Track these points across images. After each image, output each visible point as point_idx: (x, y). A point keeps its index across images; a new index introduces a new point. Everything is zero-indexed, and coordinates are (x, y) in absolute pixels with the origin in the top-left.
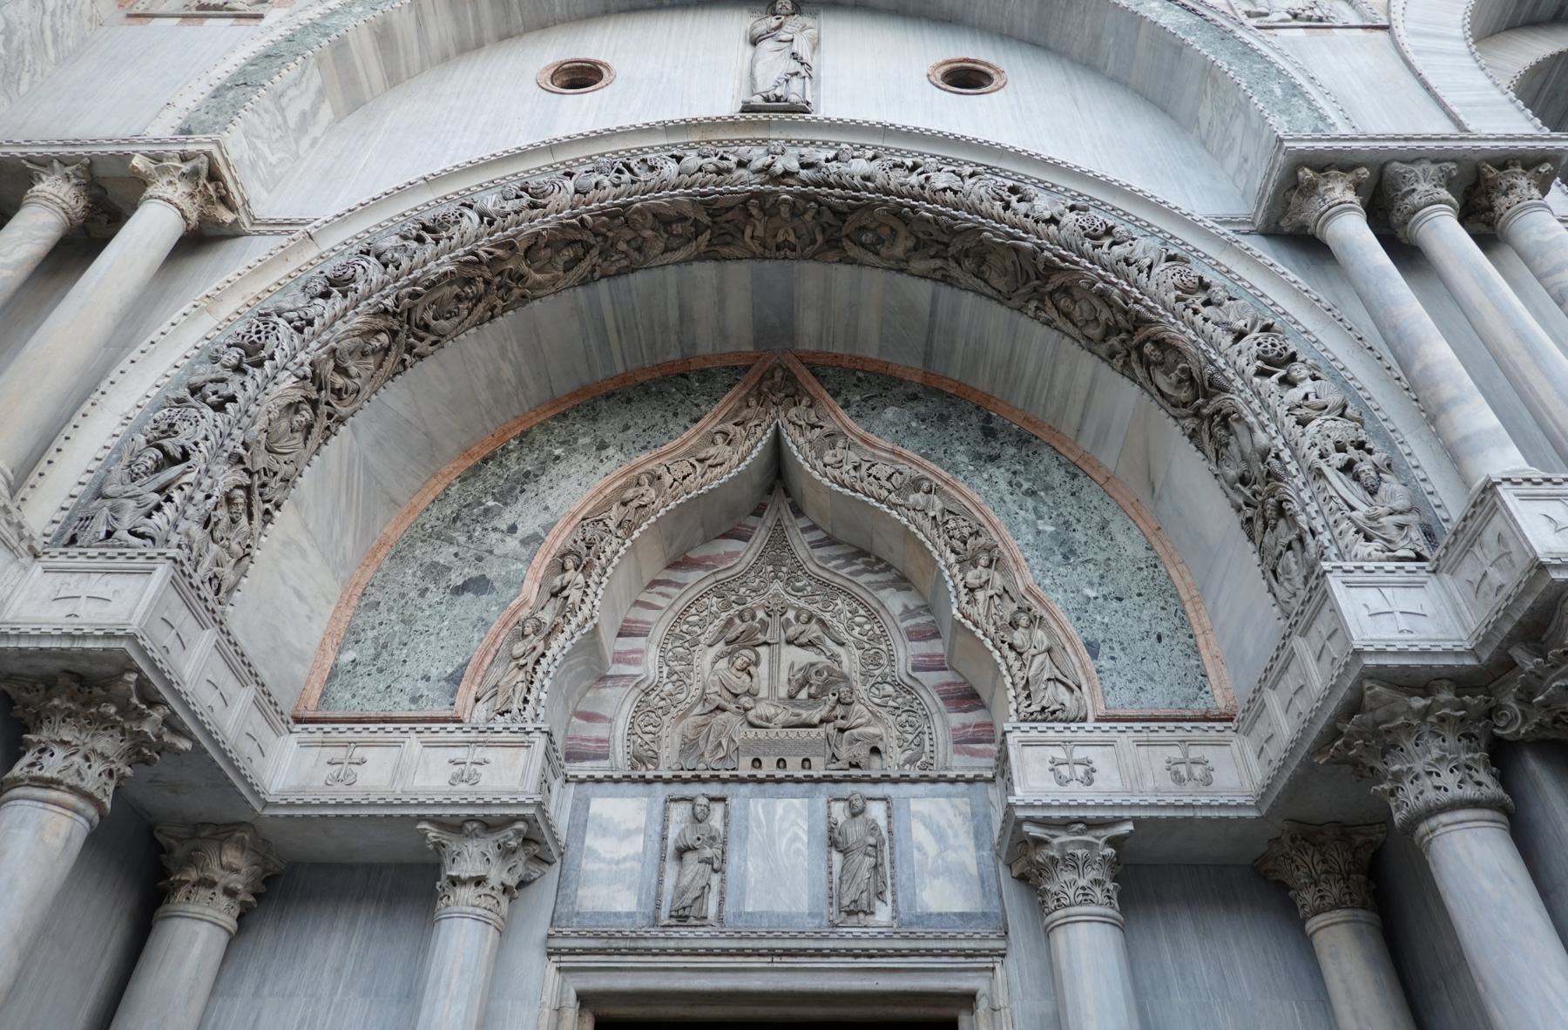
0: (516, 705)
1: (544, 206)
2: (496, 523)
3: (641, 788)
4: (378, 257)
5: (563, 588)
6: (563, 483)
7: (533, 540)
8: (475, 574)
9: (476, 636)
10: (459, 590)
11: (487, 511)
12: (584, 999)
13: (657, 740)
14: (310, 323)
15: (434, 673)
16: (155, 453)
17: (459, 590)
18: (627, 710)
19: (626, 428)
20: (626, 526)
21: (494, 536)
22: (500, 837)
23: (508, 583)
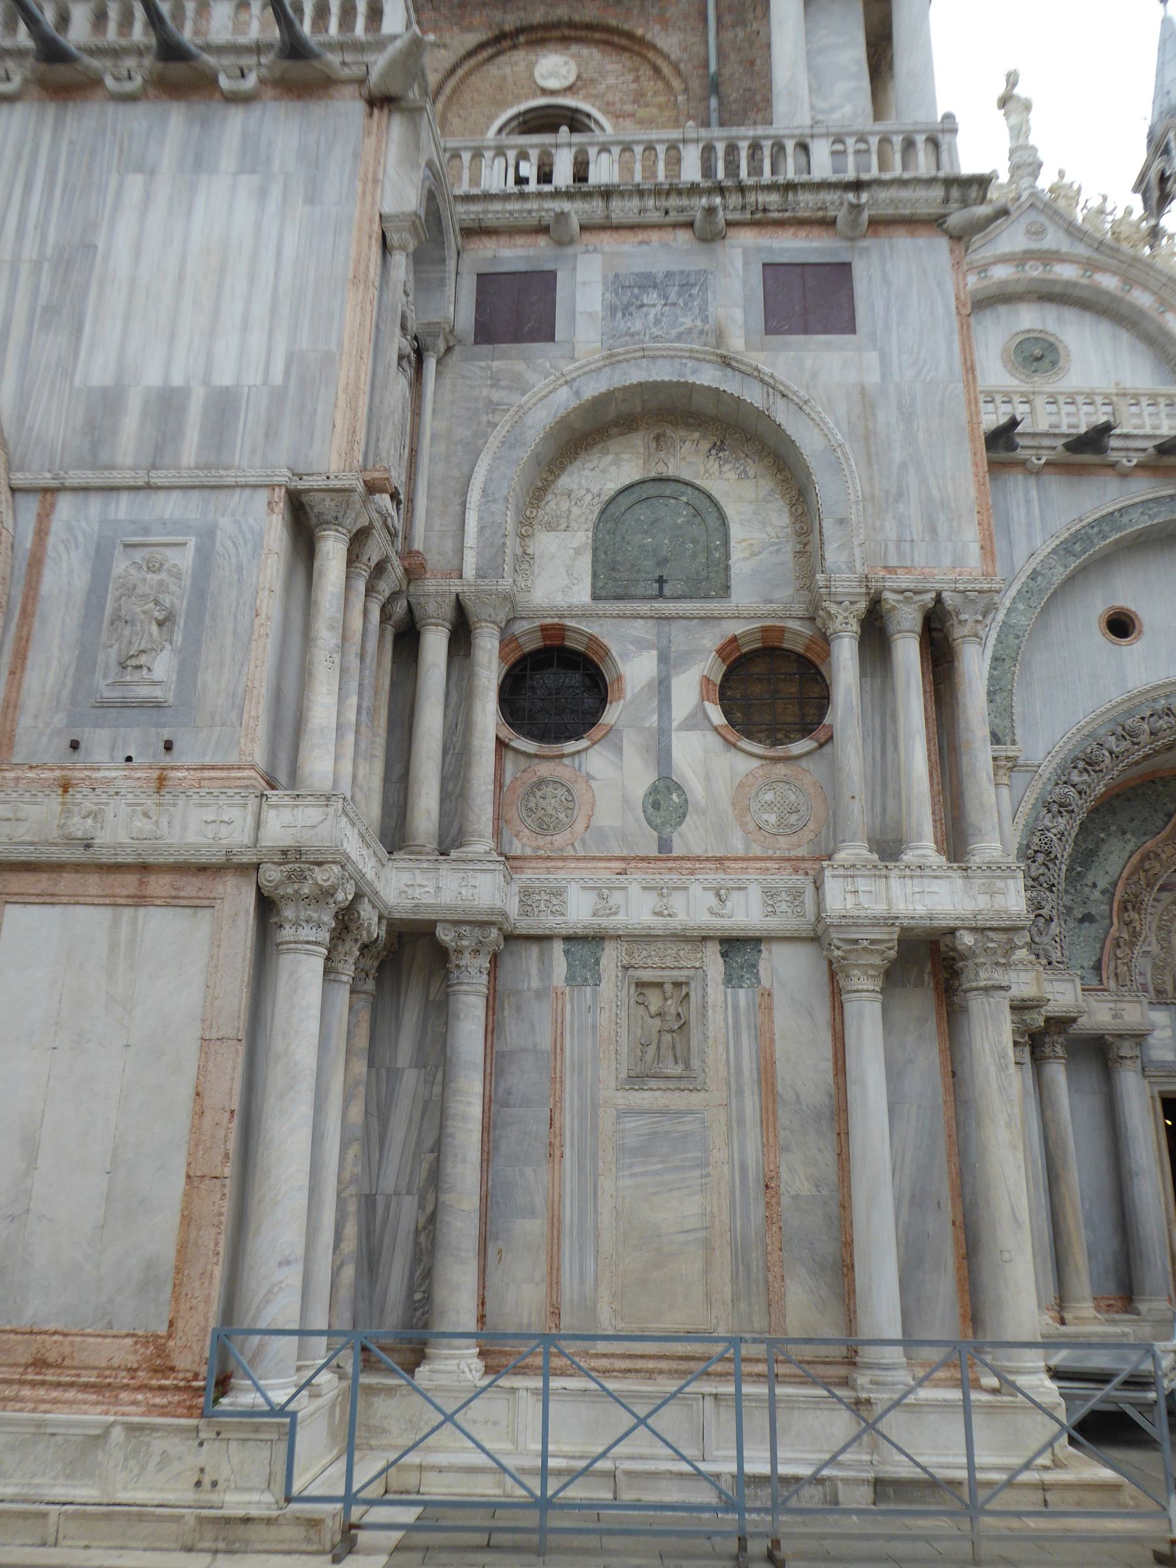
0: (1128, 983)
1: (1138, 744)
2: (1085, 881)
3: (1164, 1007)
4: (1074, 786)
5: (1131, 922)
6: (1111, 857)
7: (1109, 893)
8: (1086, 911)
9: (1098, 946)
10: (1082, 921)
11: (1079, 873)
12: (1160, 1092)
13: (1164, 982)
14: (1063, 835)
15: (1085, 965)
16: (1042, 920)
17: (1082, 921)
18: (1149, 968)
19: (1132, 820)
20: (1150, 885)
21: (1087, 890)
22: (1137, 1040)
23: (1103, 917)
